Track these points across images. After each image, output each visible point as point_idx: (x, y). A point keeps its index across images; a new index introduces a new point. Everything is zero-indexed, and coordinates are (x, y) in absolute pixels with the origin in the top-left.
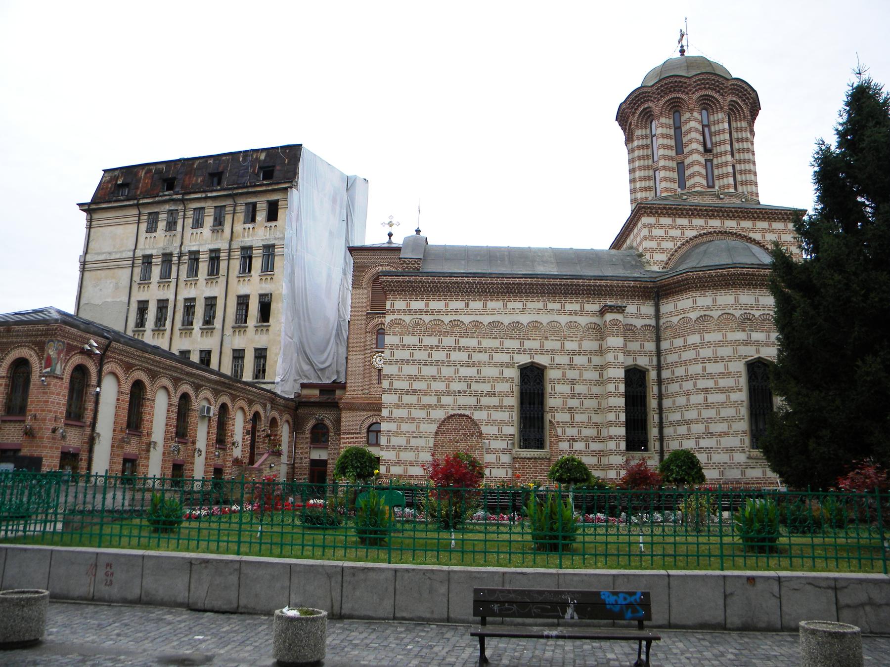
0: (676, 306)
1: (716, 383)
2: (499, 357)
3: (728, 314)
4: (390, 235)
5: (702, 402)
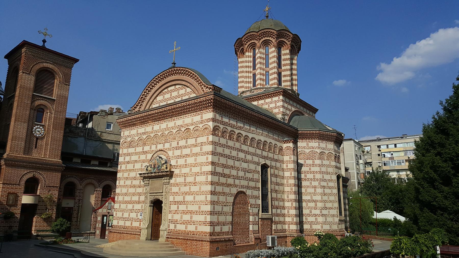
0: (308, 145)
1: (327, 184)
2: (256, 159)
3: (331, 153)
4: (44, 41)
5: (323, 193)
